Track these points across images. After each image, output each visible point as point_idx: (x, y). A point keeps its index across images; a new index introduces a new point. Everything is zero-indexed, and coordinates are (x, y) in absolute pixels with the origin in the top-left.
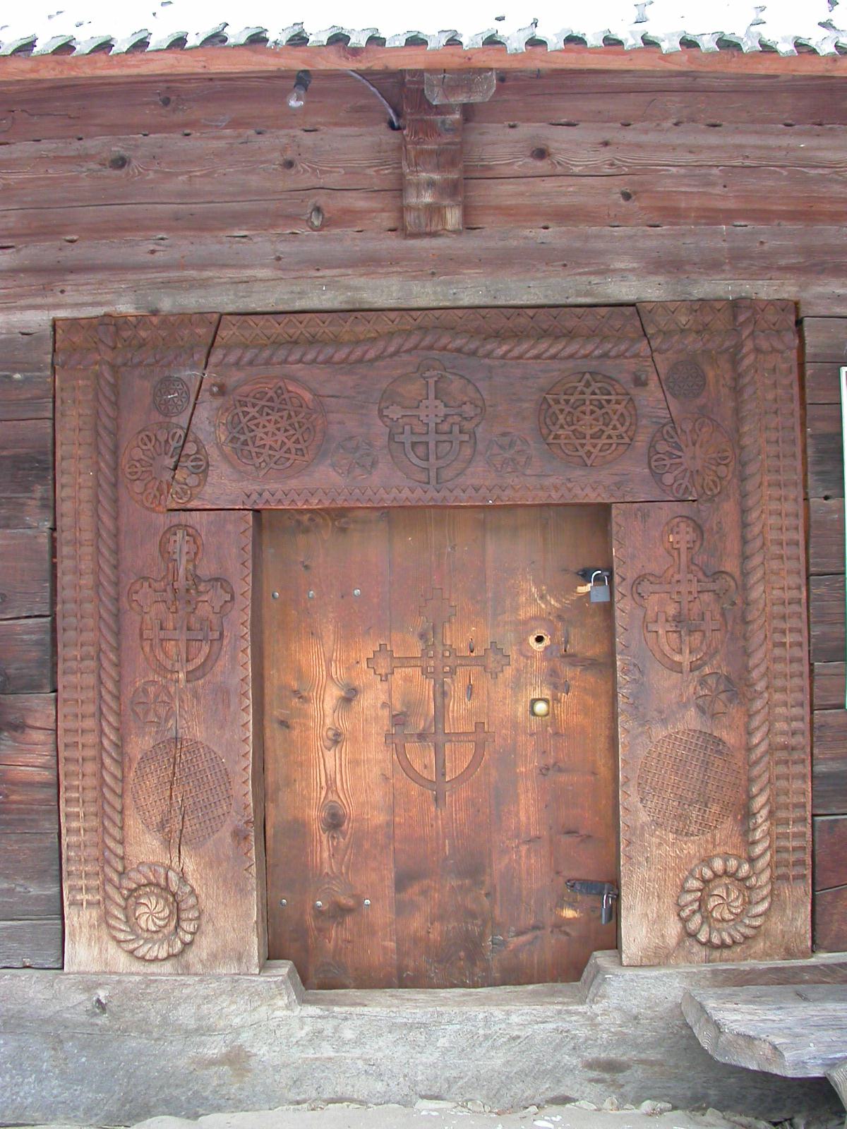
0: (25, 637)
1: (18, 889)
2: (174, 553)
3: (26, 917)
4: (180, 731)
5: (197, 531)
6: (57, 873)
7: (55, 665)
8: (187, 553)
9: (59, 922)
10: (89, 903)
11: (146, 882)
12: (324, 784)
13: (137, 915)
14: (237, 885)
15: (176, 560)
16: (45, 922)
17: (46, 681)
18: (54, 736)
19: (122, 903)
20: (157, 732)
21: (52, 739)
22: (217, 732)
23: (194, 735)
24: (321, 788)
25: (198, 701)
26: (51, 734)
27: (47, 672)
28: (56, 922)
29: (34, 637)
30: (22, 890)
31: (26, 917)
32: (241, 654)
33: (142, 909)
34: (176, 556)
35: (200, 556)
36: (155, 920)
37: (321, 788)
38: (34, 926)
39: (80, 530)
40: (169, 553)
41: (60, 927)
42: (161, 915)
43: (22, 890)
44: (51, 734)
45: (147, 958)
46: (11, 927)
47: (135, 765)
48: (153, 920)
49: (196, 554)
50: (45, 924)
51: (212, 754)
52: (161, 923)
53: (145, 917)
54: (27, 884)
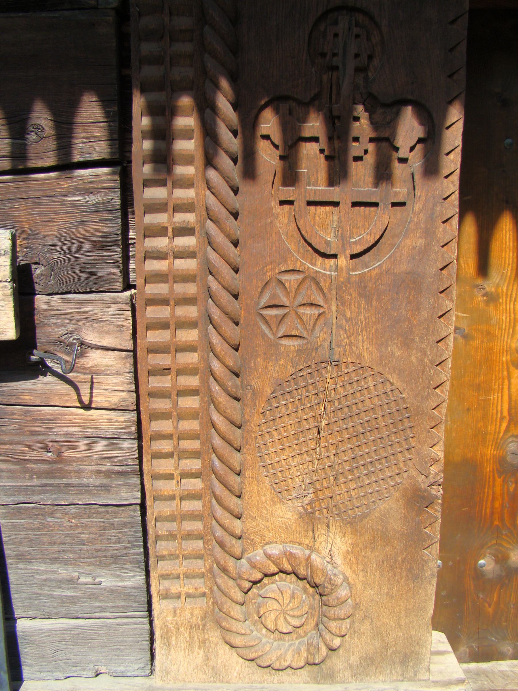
0: (77, 198)
1: (82, 579)
2: (335, 55)
3: (97, 615)
4: (337, 350)
5: (372, 18)
6: (142, 558)
7: (126, 245)
8: (357, 56)
9: (146, 620)
10: (188, 596)
11: (276, 570)
12: (505, 413)
13: (262, 613)
14: (410, 570)
15: (337, 68)
16: (125, 620)
17: (116, 271)
18: (131, 360)
19: (239, 596)
20: (299, 352)
21: (128, 367)
22: (397, 353)
23: (359, 357)
24: (502, 418)
25: (369, 301)
26: (126, 357)
27: (117, 255)
28: (142, 620)
29: (92, 199)
30: (89, 580)
31: (97, 615)
32: (442, 227)
33: (272, 605)
34: (336, 61)
35: (376, 62)
36: (288, 618)
37: (502, 418)
38: (109, 627)
39: (171, 14)
40: (323, 55)
41: (147, 626)
42: (297, 613)
43: (89, 580)
44: (126, 357)
45: (277, 666)
46: (77, 627)
47: (261, 404)
48: (285, 619)
49: (370, 57)
50: (125, 624)
51: (388, 384)
52: (297, 622)
53: (273, 616)
54: (98, 571)
